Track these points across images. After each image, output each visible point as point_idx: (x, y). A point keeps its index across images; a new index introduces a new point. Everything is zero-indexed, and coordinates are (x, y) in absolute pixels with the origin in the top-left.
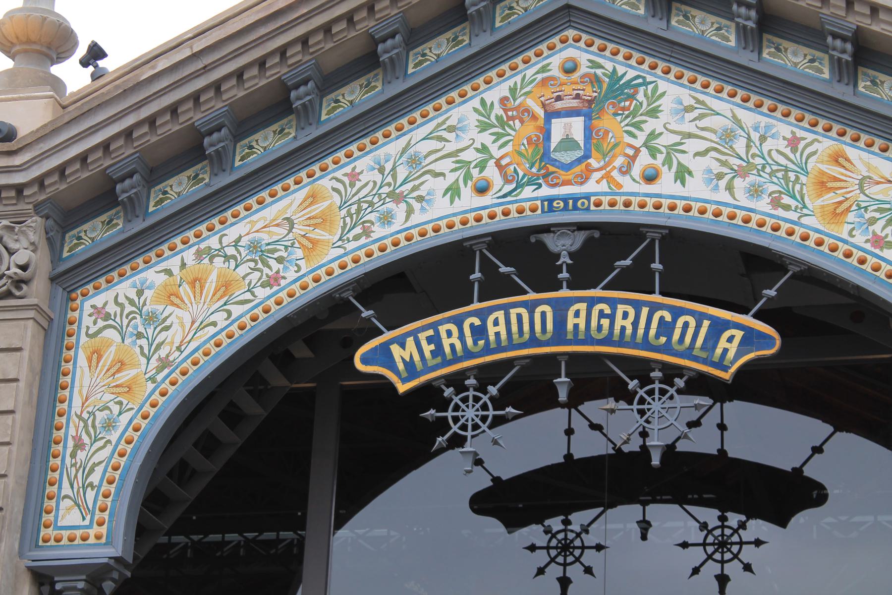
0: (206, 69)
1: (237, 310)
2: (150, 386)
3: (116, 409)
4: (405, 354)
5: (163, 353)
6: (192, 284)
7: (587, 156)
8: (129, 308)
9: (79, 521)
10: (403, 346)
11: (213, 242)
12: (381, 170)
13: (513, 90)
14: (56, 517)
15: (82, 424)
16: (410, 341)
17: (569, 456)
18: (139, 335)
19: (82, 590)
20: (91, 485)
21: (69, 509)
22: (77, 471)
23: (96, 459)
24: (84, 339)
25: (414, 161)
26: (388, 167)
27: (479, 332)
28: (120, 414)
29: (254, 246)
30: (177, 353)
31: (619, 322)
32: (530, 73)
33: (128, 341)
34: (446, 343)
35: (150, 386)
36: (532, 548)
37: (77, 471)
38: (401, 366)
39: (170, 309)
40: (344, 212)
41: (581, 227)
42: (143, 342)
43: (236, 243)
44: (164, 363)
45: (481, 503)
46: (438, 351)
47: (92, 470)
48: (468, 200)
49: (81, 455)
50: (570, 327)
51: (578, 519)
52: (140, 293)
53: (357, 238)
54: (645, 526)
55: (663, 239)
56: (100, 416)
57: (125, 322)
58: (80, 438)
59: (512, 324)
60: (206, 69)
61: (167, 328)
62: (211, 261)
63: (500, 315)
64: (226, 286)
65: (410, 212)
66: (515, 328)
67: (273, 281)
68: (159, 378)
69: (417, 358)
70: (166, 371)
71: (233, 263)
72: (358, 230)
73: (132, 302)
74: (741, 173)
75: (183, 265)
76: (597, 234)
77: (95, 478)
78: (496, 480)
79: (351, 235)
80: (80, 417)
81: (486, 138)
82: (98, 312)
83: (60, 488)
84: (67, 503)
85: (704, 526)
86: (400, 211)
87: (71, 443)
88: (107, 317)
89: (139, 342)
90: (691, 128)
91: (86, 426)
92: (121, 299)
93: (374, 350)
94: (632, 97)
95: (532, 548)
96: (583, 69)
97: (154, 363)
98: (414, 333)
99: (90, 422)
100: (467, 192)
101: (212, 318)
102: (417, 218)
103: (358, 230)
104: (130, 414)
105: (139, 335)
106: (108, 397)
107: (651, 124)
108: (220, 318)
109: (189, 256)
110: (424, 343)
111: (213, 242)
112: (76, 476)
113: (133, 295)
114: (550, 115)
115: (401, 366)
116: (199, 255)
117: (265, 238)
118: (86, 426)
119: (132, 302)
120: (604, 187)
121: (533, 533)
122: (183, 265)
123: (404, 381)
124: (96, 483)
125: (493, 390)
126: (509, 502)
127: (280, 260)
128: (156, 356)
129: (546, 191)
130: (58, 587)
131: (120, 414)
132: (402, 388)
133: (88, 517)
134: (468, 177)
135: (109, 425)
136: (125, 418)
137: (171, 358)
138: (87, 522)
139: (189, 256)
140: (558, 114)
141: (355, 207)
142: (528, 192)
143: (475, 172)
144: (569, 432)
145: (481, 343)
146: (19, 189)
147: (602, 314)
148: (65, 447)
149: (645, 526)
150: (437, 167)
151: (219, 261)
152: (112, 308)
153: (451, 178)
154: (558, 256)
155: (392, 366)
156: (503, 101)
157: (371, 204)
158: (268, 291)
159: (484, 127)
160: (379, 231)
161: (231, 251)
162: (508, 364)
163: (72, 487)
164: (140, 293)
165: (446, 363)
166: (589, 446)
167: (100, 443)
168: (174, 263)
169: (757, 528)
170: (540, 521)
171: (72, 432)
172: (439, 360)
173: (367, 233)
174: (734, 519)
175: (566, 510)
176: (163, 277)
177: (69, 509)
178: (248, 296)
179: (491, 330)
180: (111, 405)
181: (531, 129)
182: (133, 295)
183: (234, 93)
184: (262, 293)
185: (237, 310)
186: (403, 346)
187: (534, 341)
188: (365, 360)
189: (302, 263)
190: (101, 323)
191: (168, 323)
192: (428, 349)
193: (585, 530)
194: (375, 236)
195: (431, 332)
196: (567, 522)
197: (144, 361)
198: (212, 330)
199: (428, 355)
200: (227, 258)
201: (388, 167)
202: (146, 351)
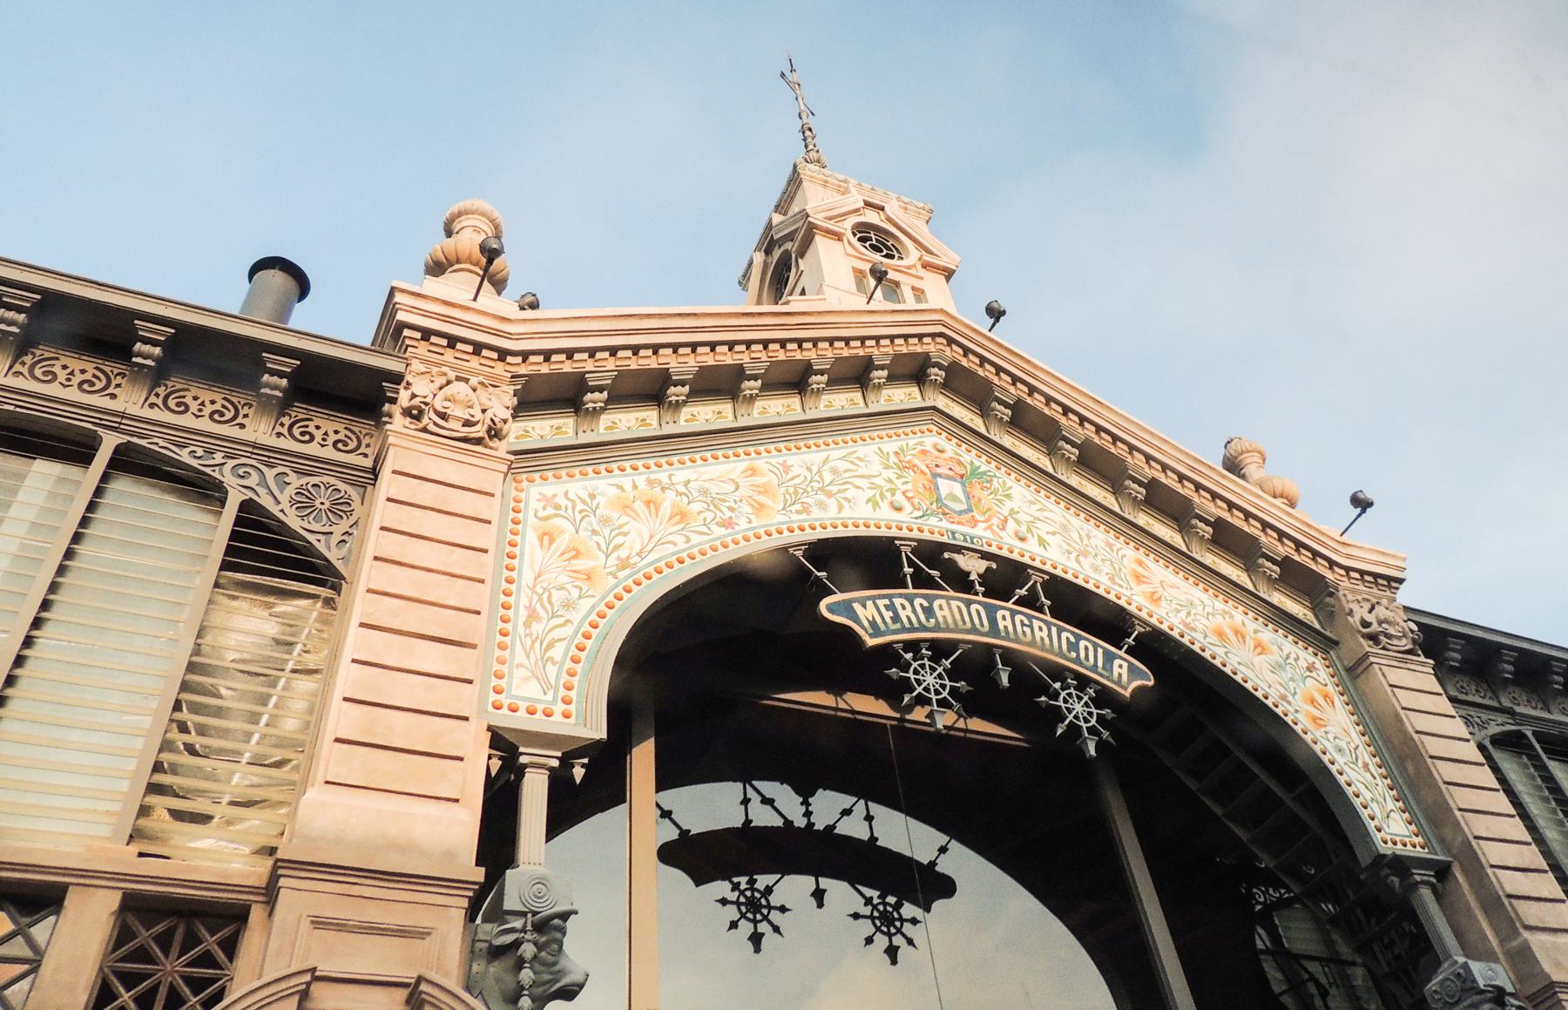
0: (694, 330)
1: (695, 539)
2: (612, 581)
3: (575, 593)
4: (870, 614)
5: (623, 553)
6: (648, 503)
7: (970, 510)
8: (580, 506)
9: (538, 694)
10: (864, 606)
11: (663, 476)
12: (809, 469)
13: (902, 449)
14: (510, 684)
15: (535, 598)
16: (869, 603)
17: (748, 822)
18: (594, 532)
19: (551, 769)
20: (551, 659)
21: (526, 679)
22: (533, 642)
23: (556, 634)
24: (531, 519)
25: (834, 471)
26: (815, 469)
27: (929, 611)
28: (580, 597)
29: (704, 492)
30: (637, 559)
31: (1038, 634)
32: (911, 443)
33: (582, 534)
34: (902, 614)
35: (612, 581)
36: (724, 902)
37: (533, 642)
38: (866, 624)
39: (624, 519)
40: (783, 490)
41: (985, 556)
42: (600, 539)
43: (686, 484)
44: (624, 564)
45: (668, 854)
46: (896, 618)
47: (551, 645)
48: (885, 513)
49: (537, 628)
50: (1001, 627)
51: (763, 881)
52: (592, 496)
53: (798, 512)
54: (819, 895)
55: (1044, 584)
56: (556, 595)
57: (578, 517)
58: (534, 611)
59: (953, 615)
60: (694, 330)
61: (625, 534)
62: (663, 489)
63: (943, 602)
64: (681, 516)
65: (840, 508)
66: (958, 617)
67: (728, 524)
68: (622, 575)
69: (879, 620)
70: (627, 572)
71: (685, 500)
72: (798, 507)
73: (583, 502)
74: (1085, 554)
75: (635, 487)
76: (994, 566)
77: (557, 652)
78: (684, 834)
79: (793, 508)
80: (533, 589)
81: (890, 474)
82: (548, 501)
83: (512, 654)
84: (523, 673)
85: (868, 901)
86: (832, 503)
87: (523, 614)
88: (558, 507)
89: (595, 538)
90: (1038, 514)
91: (540, 599)
92: (571, 495)
93: (838, 603)
94: (990, 482)
95: (724, 902)
96: (949, 454)
97: (613, 561)
98: (873, 598)
99: (545, 597)
100: (885, 505)
101: (671, 538)
102: (846, 513)
103: (798, 507)
104: (592, 601)
105: (594, 532)
106: (563, 579)
107: (1009, 505)
108: (680, 540)
109: (641, 480)
110: (883, 610)
111: (663, 476)
112: (532, 646)
113: (585, 496)
114: (935, 475)
115: (866, 624)
116: (650, 483)
117: (713, 489)
118: (540, 599)
119: (583, 502)
120: (988, 534)
121: (722, 888)
122: (635, 487)
123: (871, 636)
124: (558, 658)
125: (947, 663)
126: (695, 856)
127: (731, 509)
128: (615, 555)
129: (945, 524)
130: (523, 760)
131: (580, 597)
132: (871, 642)
133: (551, 693)
134: (882, 496)
135: (568, 605)
136: (586, 604)
137: (632, 561)
138: (550, 697)
139: (641, 480)
140: (940, 476)
141: (791, 490)
142: (933, 521)
143: (888, 495)
144: (746, 801)
145: (932, 621)
146: (503, 354)
147: (1023, 624)
148: (517, 614)
149: (819, 895)
150: (858, 481)
151: (670, 494)
152: (561, 501)
153: (870, 493)
154: (968, 574)
155: (857, 620)
156: (896, 453)
157: (805, 491)
158: (723, 531)
159: (887, 467)
160: (816, 513)
161: (682, 489)
162: (954, 644)
163: (528, 656)
164: (592, 496)
165: (903, 630)
166: (764, 817)
167: (560, 621)
168: (626, 482)
169: (909, 910)
170: (726, 877)
171: (524, 601)
172: (898, 626)
173: (806, 510)
174: (891, 900)
175: (751, 871)
176: (615, 491)
177: (526, 679)
178: (704, 529)
179: (939, 614)
180: (569, 586)
181: (922, 480)
182: (585, 496)
183: (707, 358)
184: (720, 531)
185: (695, 539)
186: (864, 606)
187: (974, 630)
188: (830, 609)
189: (753, 517)
190: (550, 511)
191: (625, 529)
192: (888, 615)
193: (769, 890)
194: (814, 515)
195: (887, 602)
196: (752, 882)
197: (602, 556)
198: (672, 549)
199: (888, 620)
200: (679, 494)
201: (815, 469)
202: (604, 547)
